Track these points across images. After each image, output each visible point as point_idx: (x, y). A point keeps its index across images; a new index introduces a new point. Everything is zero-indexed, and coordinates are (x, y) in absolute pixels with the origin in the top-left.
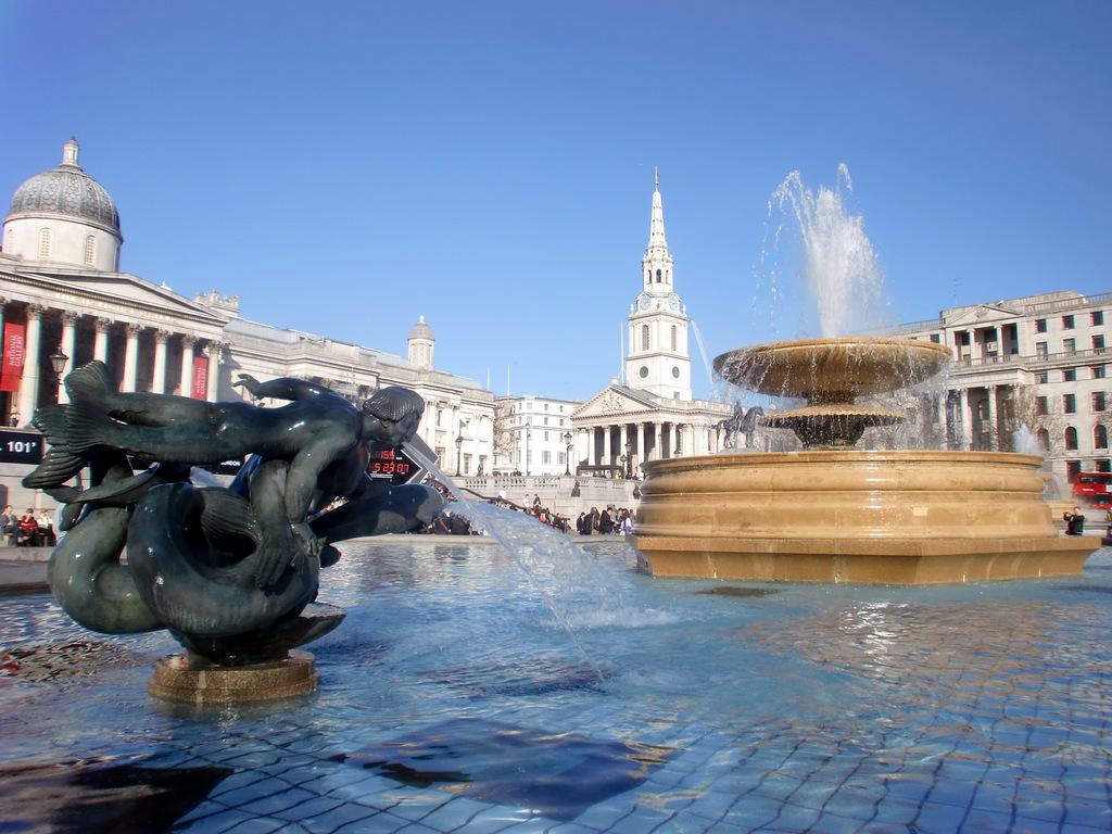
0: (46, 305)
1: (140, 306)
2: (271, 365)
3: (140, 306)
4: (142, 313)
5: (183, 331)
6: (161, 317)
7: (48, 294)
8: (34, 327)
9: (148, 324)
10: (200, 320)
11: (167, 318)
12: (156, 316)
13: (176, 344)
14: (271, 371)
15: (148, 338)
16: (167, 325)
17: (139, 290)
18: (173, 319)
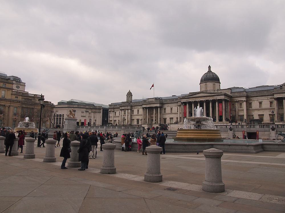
0: (188, 101)
1: (204, 97)
2: (268, 97)
3: (204, 97)
4: (205, 98)
5: (214, 99)
6: (209, 97)
7: (189, 99)
8: (187, 105)
9: (206, 99)
10: (218, 95)
11: (210, 97)
12: (208, 97)
13: (214, 102)
14: (269, 98)
15: (207, 102)
16: (211, 99)
17: (204, 94)
18: (212, 97)
